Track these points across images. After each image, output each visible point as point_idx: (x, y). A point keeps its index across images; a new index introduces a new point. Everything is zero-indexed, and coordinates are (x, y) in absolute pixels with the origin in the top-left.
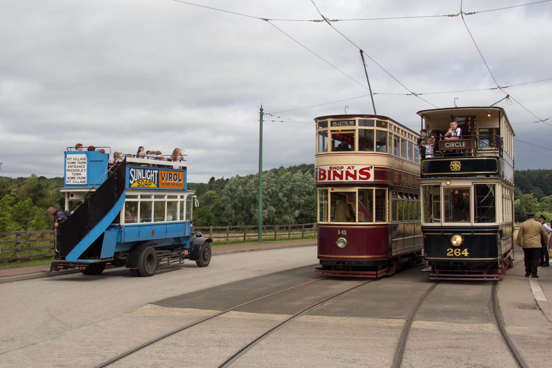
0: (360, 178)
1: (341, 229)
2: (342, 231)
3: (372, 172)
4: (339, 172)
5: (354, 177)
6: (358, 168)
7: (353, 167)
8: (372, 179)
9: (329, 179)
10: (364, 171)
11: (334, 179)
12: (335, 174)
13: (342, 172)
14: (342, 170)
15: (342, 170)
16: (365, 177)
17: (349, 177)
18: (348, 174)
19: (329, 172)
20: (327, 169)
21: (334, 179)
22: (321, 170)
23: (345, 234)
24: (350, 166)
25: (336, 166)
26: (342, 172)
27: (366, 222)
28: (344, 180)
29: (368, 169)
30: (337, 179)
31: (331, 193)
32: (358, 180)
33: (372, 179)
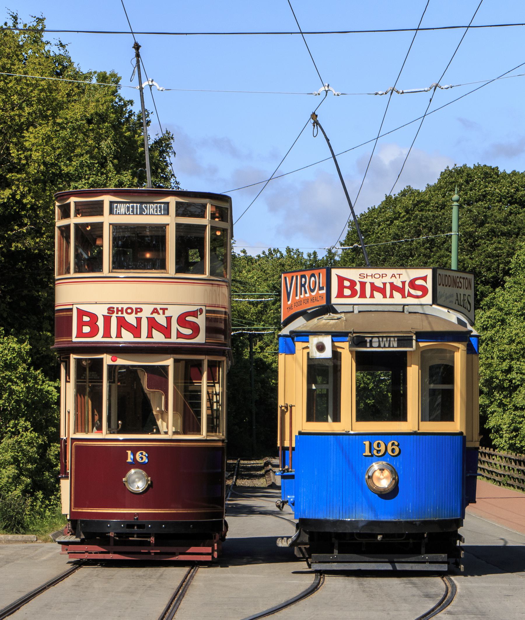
0: (180, 335)
1: (135, 450)
2: (138, 455)
3: (201, 321)
4: (131, 319)
5: (166, 331)
6: (175, 312)
7: (164, 310)
8: (201, 338)
9: (107, 333)
10: (188, 319)
11: (119, 335)
12: (122, 323)
13: (139, 320)
14: (139, 315)
15: (139, 315)
16: (188, 332)
17: (154, 332)
18: (153, 324)
19: (107, 320)
20: (101, 311)
21: (119, 335)
22: (81, 313)
23: (145, 460)
24: (158, 307)
25: (125, 307)
26: (139, 320)
27: (185, 433)
28: (144, 338)
29: (194, 314)
30: (127, 337)
31: (110, 367)
32: (174, 339)
33: (201, 338)
